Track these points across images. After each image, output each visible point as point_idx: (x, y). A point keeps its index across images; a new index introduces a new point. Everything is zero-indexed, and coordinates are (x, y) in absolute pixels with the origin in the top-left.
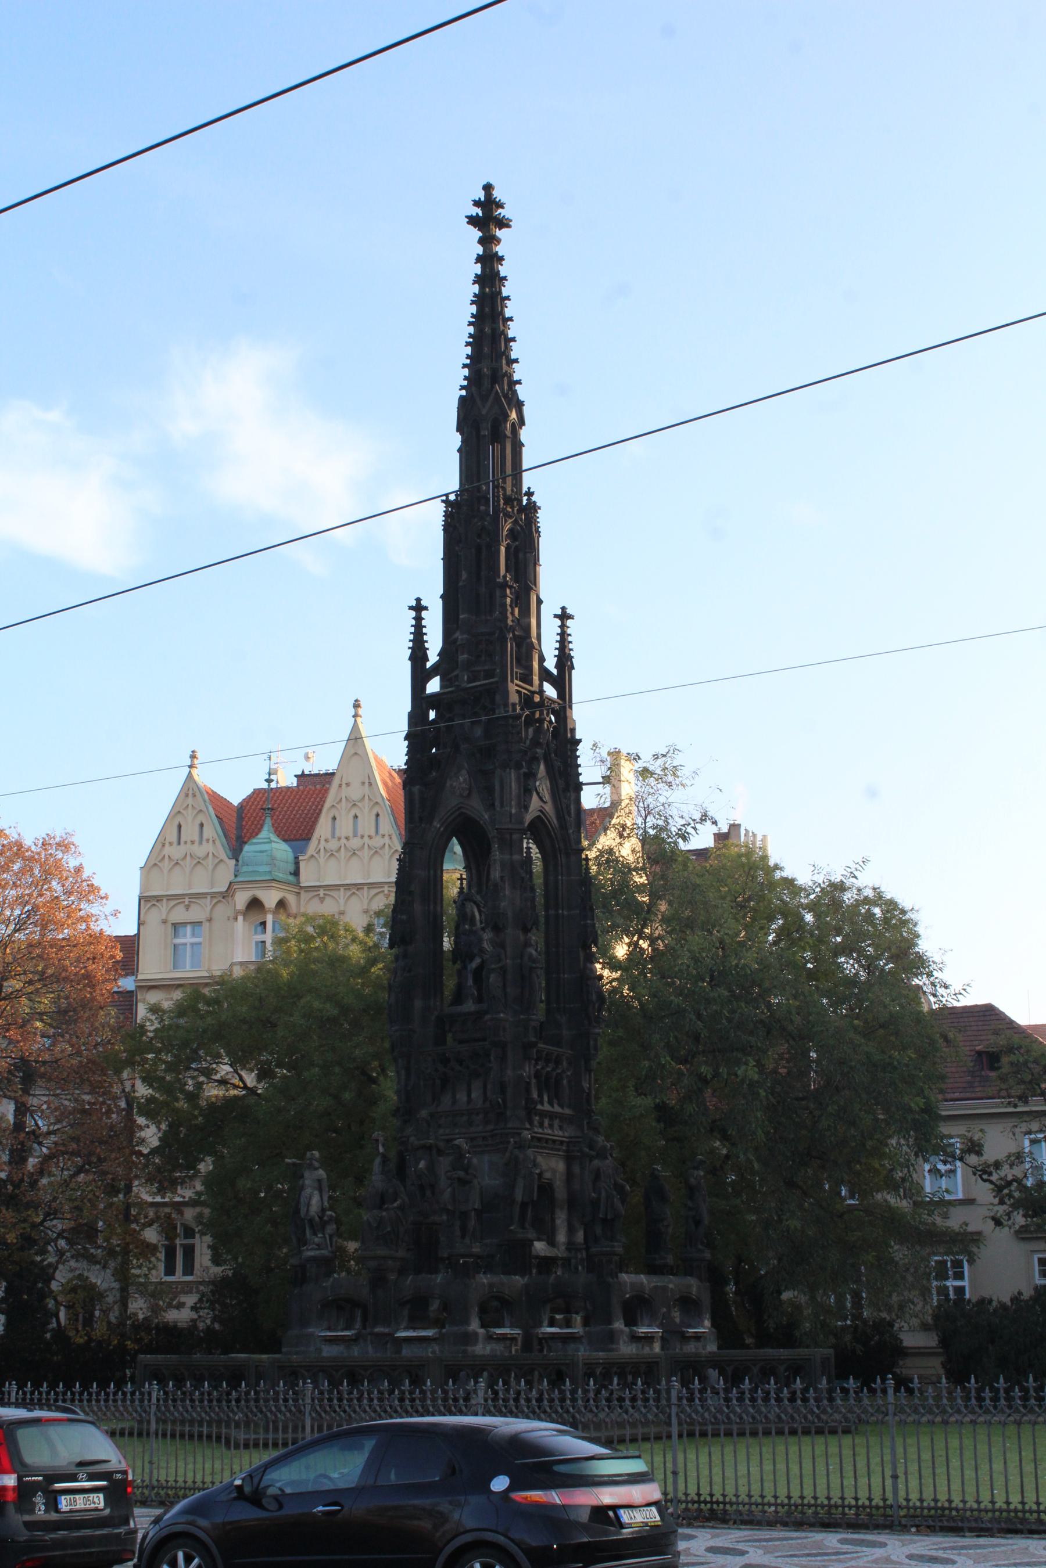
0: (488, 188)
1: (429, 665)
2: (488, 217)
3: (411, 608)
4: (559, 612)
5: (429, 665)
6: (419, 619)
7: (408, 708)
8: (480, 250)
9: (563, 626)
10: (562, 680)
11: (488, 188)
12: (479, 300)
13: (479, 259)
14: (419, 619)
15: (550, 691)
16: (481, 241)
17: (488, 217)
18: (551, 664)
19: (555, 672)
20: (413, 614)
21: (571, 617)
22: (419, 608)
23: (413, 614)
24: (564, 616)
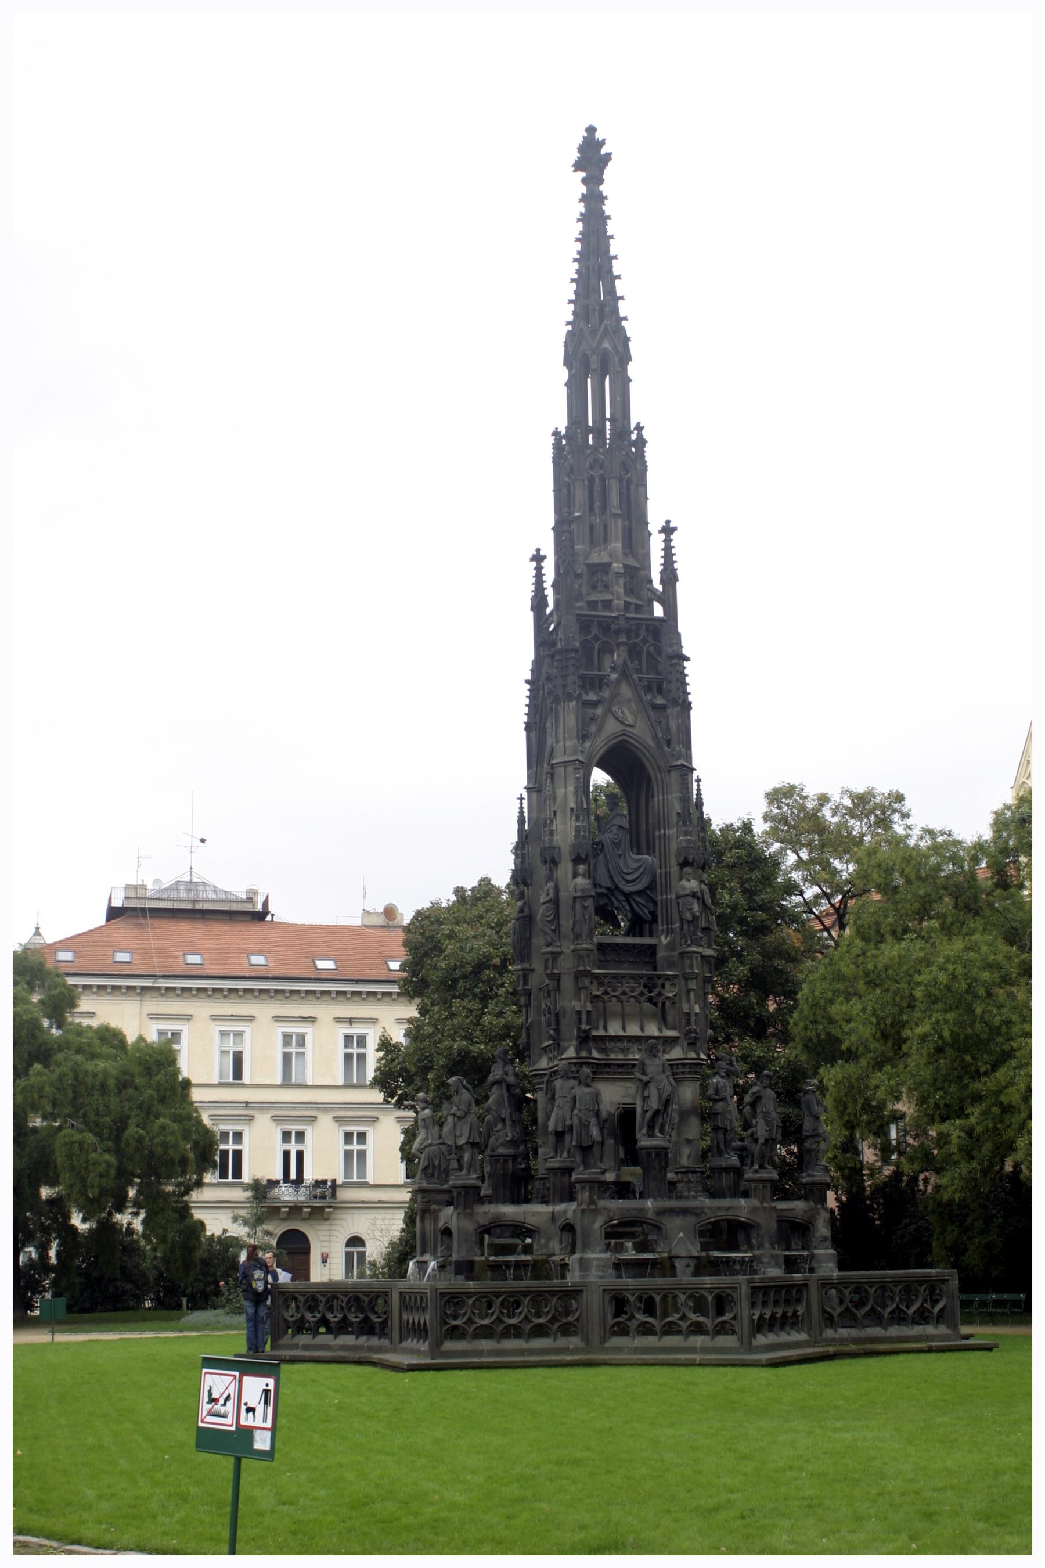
0: (591, 130)
1: (548, 611)
2: (592, 158)
3: (532, 560)
4: (672, 525)
5: (548, 611)
6: (539, 569)
7: (533, 657)
8: (583, 189)
9: (668, 541)
10: (669, 600)
11: (591, 130)
12: (584, 239)
13: (584, 198)
14: (539, 569)
15: (658, 611)
16: (584, 181)
17: (592, 158)
18: (657, 585)
19: (660, 588)
20: (534, 564)
21: (675, 529)
22: (538, 558)
23: (534, 564)
24: (668, 530)
